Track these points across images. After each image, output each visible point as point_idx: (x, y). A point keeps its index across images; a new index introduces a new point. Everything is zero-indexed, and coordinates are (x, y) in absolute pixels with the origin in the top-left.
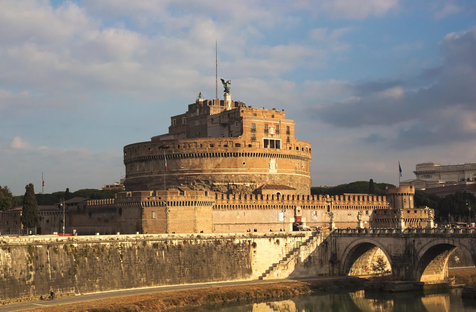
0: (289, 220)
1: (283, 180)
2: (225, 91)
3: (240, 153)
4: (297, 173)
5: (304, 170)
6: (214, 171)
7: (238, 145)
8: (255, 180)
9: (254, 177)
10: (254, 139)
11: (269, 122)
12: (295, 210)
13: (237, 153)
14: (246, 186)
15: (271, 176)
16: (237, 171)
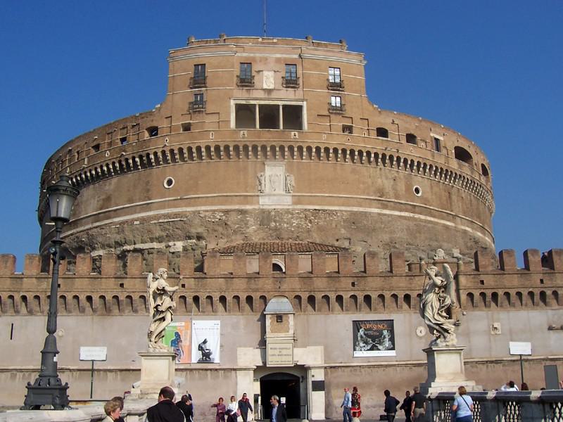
0: (234, 357)
1: (320, 229)
3: (155, 154)
4: (385, 205)
5: (425, 200)
6: (97, 217)
7: (153, 131)
8: (200, 230)
9: (197, 221)
10: (197, 106)
11: (258, 55)
12: (263, 317)
13: (148, 155)
14: (172, 250)
15: (265, 217)
16: (148, 207)
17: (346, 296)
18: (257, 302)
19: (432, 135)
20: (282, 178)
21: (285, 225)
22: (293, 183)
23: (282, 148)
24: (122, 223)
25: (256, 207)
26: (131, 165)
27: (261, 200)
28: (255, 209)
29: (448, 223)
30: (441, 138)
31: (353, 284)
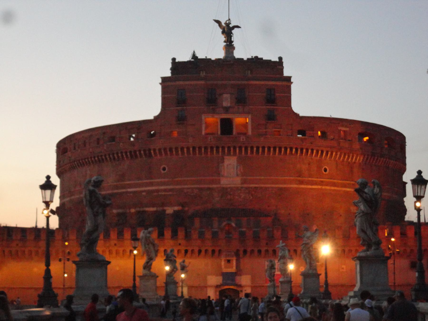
2: (225, 42)
3: (154, 150)
4: (301, 183)
6: (117, 187)
11: (220, 82)
13: (150, 150)
15: (224, 191)
16: (151, 184)
17: (263, 250)
18: (217, 253)
19: (340, 128)
20: (236, 167)
21: (237, 197)
22: (242, 170)
23: (235, 148)
24: (134, 192)
25: (218, 186)
26: (138, 155)
27: (222, 182)
28: (217, 188)
29: (348, 189)
30: (347, 129)
31: (267, 244)
